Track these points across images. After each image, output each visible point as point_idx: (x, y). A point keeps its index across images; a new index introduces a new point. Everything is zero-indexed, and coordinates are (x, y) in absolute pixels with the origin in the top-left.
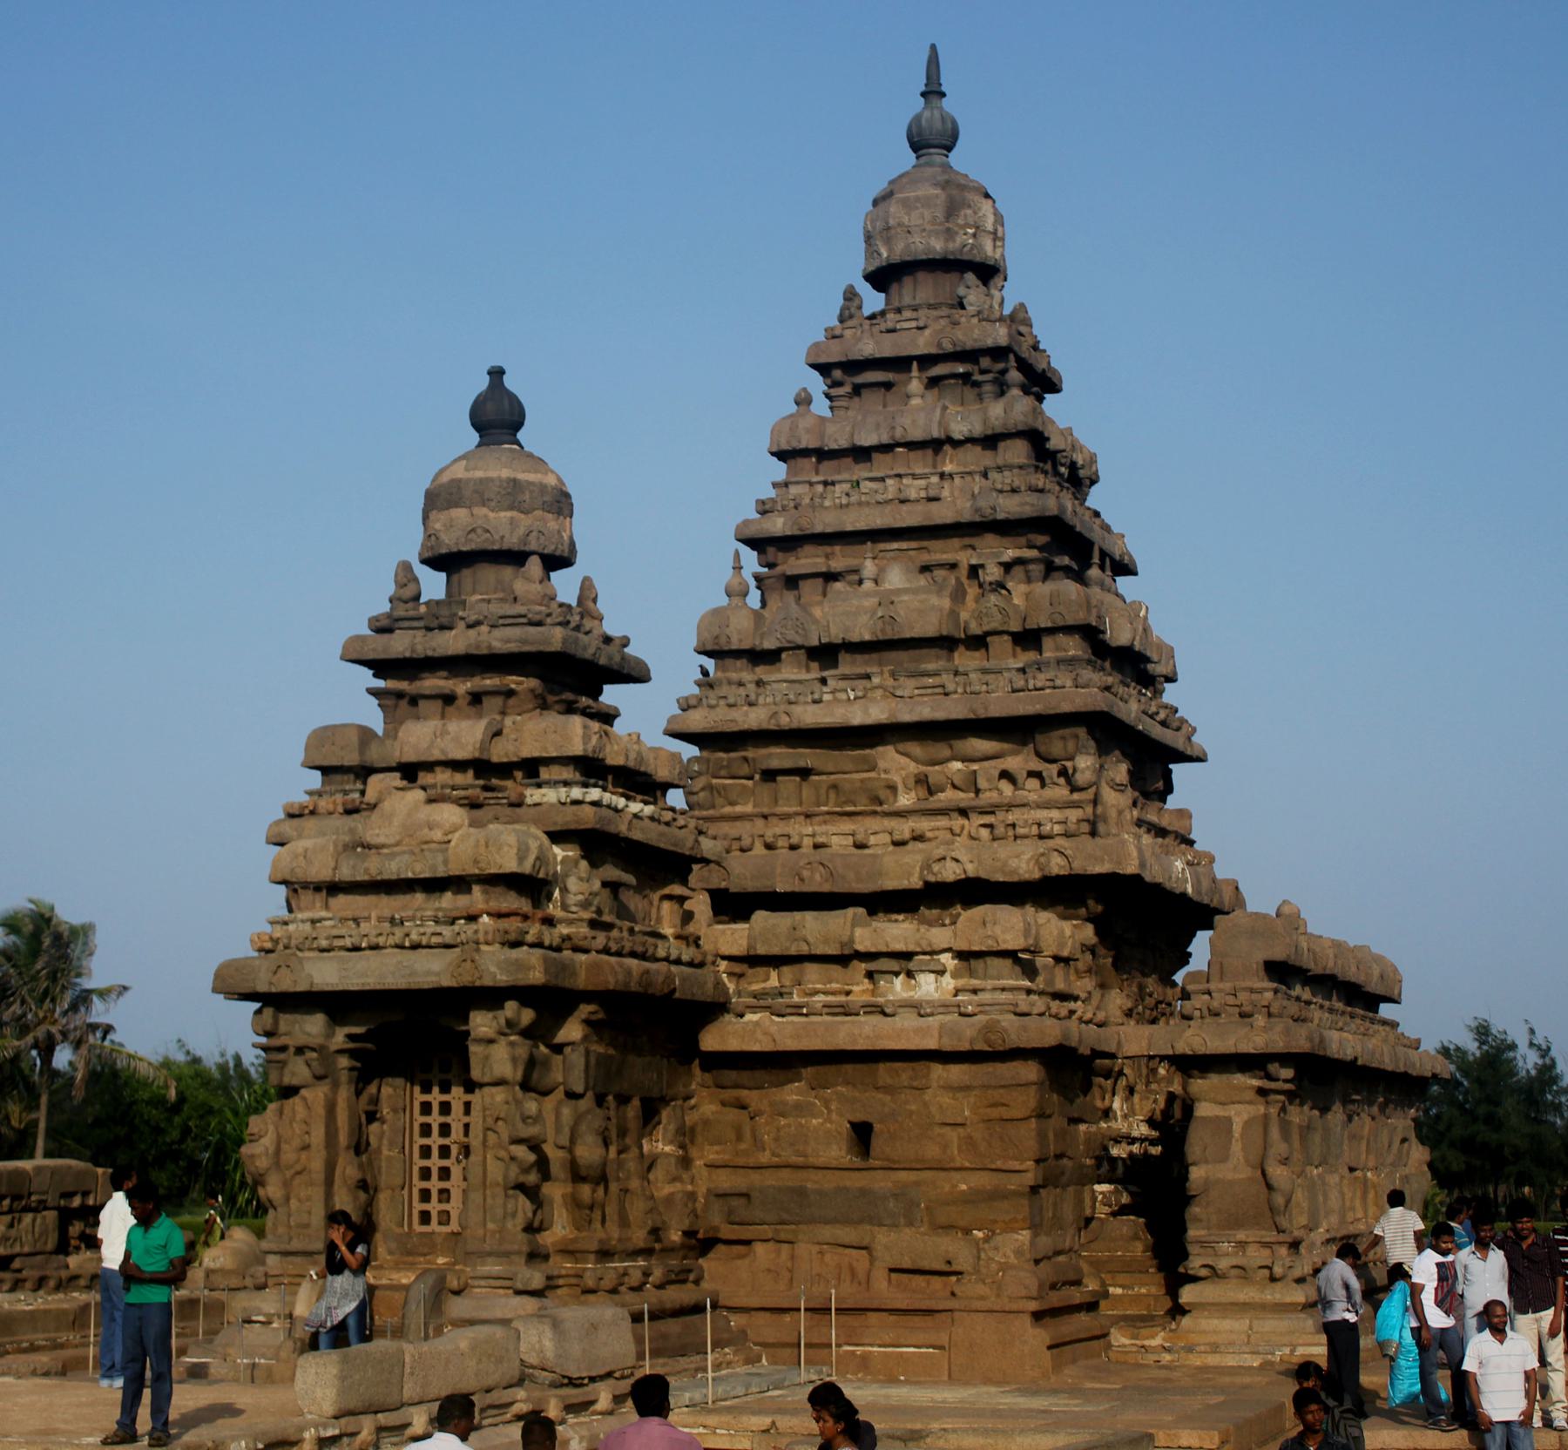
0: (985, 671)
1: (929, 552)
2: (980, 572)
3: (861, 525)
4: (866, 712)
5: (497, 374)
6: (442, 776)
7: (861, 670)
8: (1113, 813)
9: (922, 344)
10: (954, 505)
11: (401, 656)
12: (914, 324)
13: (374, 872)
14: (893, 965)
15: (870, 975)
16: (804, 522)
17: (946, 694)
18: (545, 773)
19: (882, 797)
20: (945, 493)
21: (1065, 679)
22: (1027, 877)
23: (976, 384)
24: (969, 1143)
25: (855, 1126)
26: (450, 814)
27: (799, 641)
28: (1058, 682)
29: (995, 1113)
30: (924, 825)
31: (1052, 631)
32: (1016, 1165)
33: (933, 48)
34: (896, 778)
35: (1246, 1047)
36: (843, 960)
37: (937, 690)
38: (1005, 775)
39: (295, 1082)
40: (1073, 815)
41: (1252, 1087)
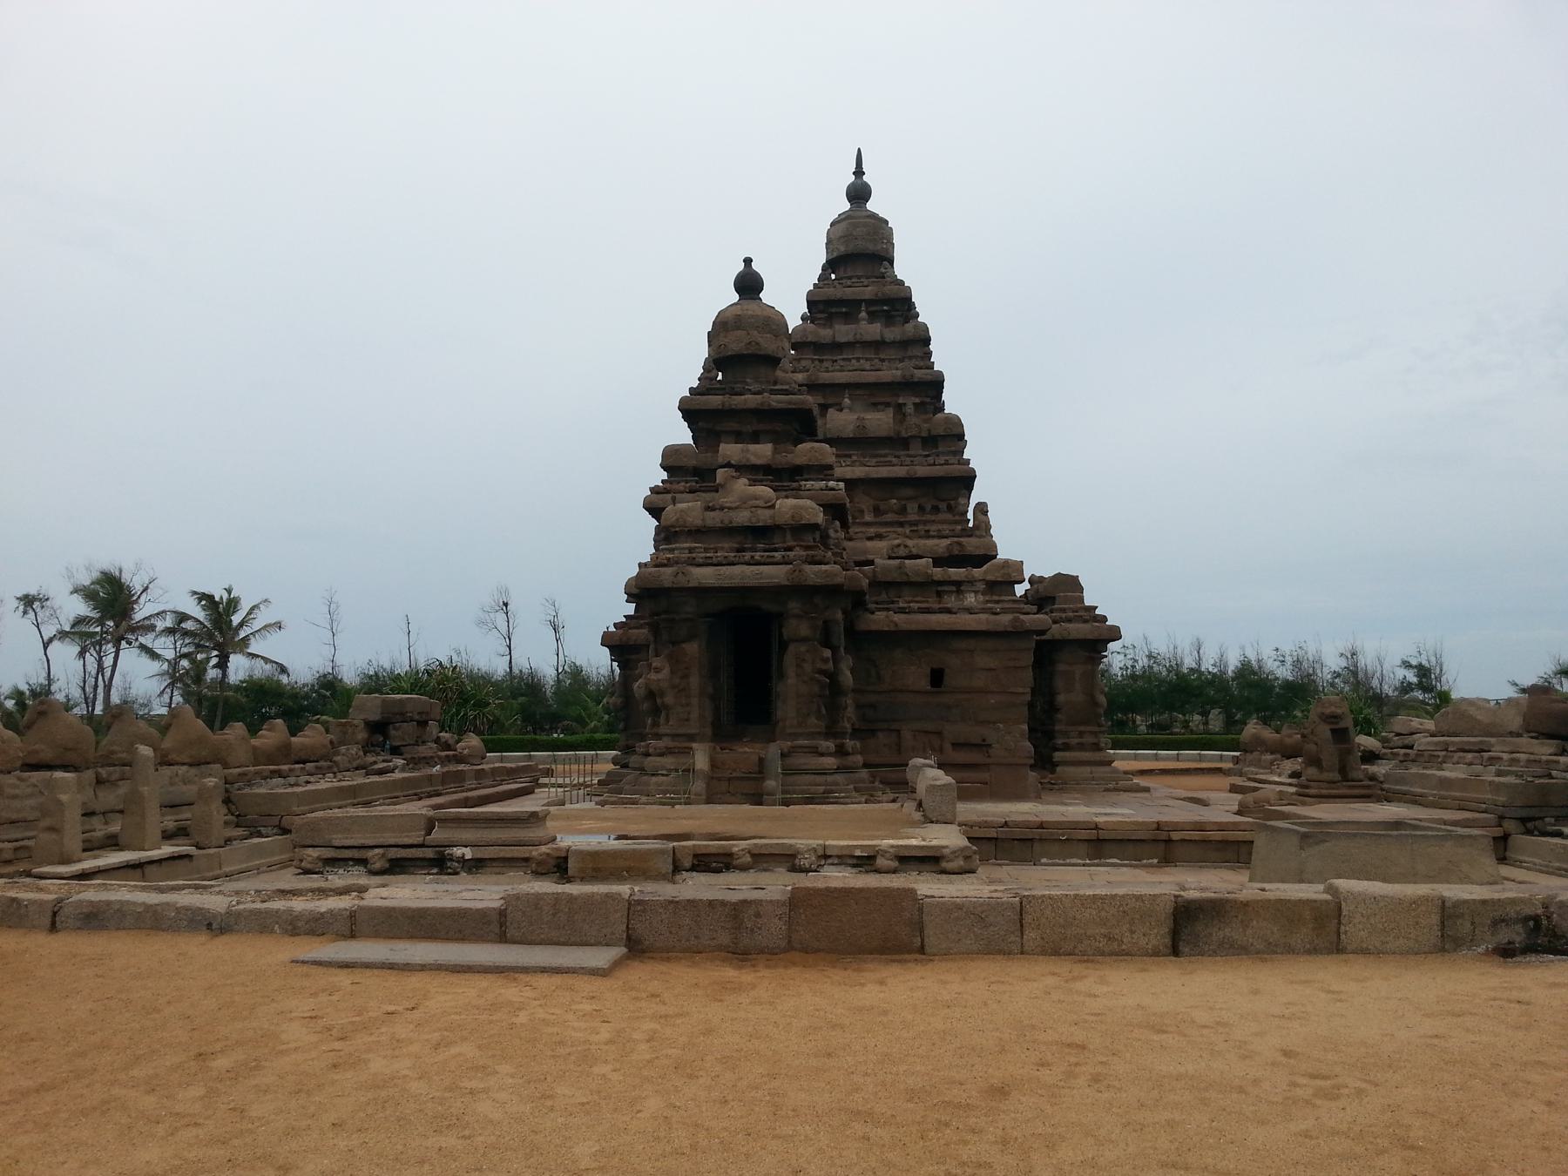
7: (847, 453)
11: (715, 408)
13: (726, 522)
14: (954, 589)
15: (939, 594)
16: (813, 378)
17: (893, 465)
21: (952, 460)
25: (933, 671)
28: (950, 462)
30: (882, 530)
32: (1021, 690)
33: (859, 149)
34: (864, 507)
40: (959, 527)
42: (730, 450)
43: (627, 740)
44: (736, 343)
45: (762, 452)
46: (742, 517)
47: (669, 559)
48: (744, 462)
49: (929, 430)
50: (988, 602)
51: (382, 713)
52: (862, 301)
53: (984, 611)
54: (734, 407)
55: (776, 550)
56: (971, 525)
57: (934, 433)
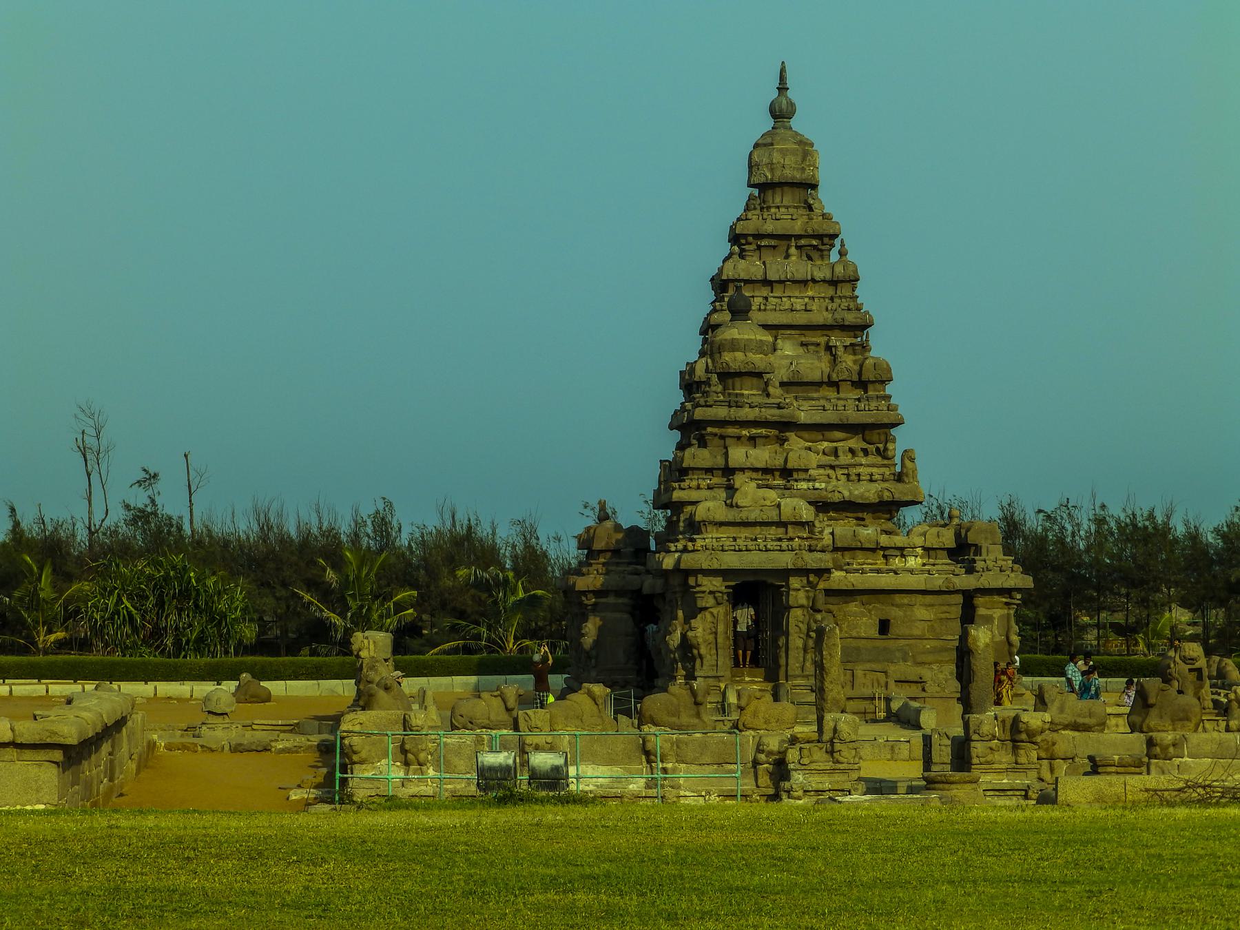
0: (839, 399)
1: (805, 336)
2: (833, 349)
3: (775, 323)
9: (797, 227)
12: (790, 217)
14: (898, 553)
15: (885, 556)
18: (795, 476)
20: (814, 308)
24: (932, 628)
26: (772, 495)
29: (943, 616)
31: (873, 382)
32: (950, 637)
33: (783, 63)
35: (1006, 585)
37: (820, 408)
38: (851, 451)
39: (707, 606)
40: (887, 472)
41: (1002, 602)
42: (738, 455)
43: (597, 675)
45: (763, 455)
46: (754, 516)
47: (702, 546)
48: (749, 465)
49: (860, 374)
50: (924, 565)
53: (922, 572)
54: (738, 419)
55: (780, 540)
56: (898, 469)
57: (864, 378)
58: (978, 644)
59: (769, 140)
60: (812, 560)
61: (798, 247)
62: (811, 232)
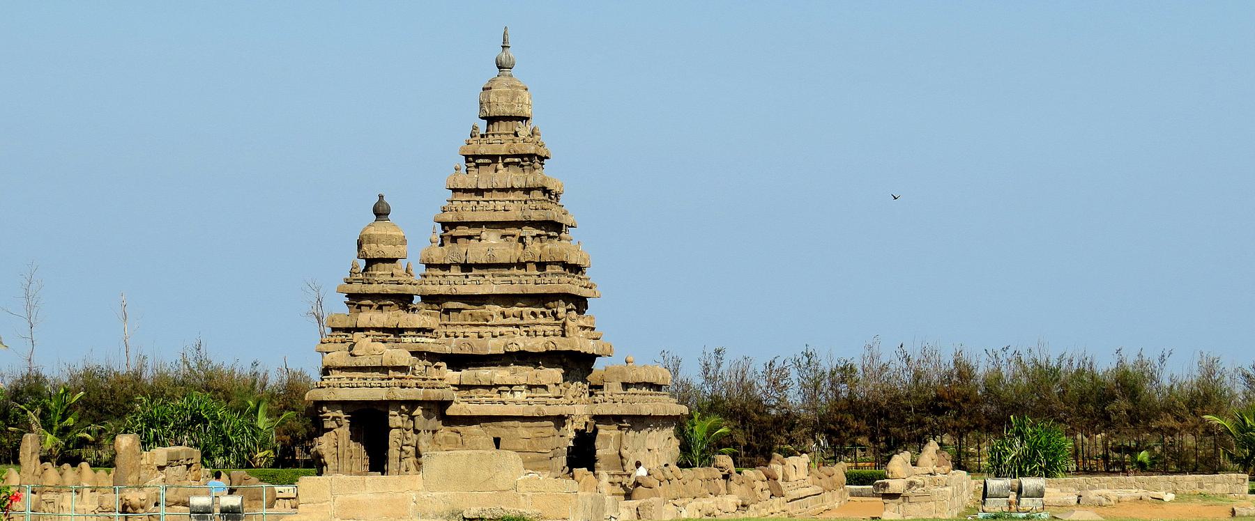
0: (526, 275)
3: (481, 220)
4: (484, 289)
5: (381, 197)
6: (372, 332)
8: (571, 329)
9: (503, 150)
10: (515, 214)
12: (499, 141)
14: (509, 389)
15: (499, 392)
19: (488, 319)
22: (541, 351)
23: (522, 166)
24: (531, 445)
25: (494, 438)
27: (459, 261)
30: (504, 330)
31: (550, 263)
35: (615, 413)
36: (489, 387)
44: (372, 251)
46: (363, 362)
51: (168, 460)
52: (498, 156)
58: (121, 447)
59: (489, 86)
60: (400, 394)
61: (506, 165)
62: (513, 153)
